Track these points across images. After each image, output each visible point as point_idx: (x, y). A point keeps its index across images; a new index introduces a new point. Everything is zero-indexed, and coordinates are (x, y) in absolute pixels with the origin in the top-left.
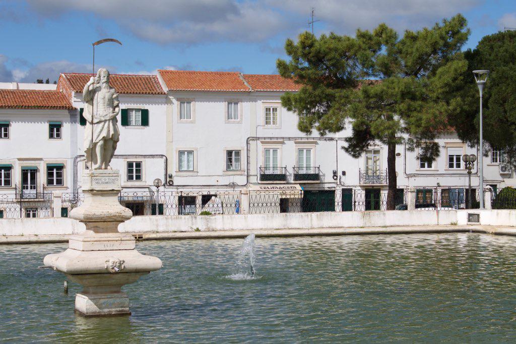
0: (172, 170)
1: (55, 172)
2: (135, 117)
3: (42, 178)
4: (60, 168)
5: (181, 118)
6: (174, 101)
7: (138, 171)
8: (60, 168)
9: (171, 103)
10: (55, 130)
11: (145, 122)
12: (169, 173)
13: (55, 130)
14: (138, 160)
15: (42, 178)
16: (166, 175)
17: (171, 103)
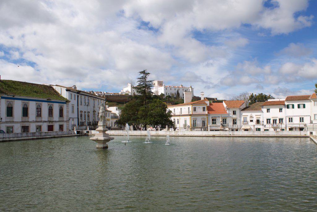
0: (312, 119)
1: (281, 120)
2: (301, 106)
3: (278, 122)
4: (282, 119)
5: (314, 105)
6: (312, 101)
7: (301, 120)
8: (282, 119)
9: (311, 102)
10: (281, 110)
11: (304, 107)
12: (311, 120)
13: (281, 110)
14: (303, 117)
15: (278, 122)
16: (311, 121)
17: (311, 102)
